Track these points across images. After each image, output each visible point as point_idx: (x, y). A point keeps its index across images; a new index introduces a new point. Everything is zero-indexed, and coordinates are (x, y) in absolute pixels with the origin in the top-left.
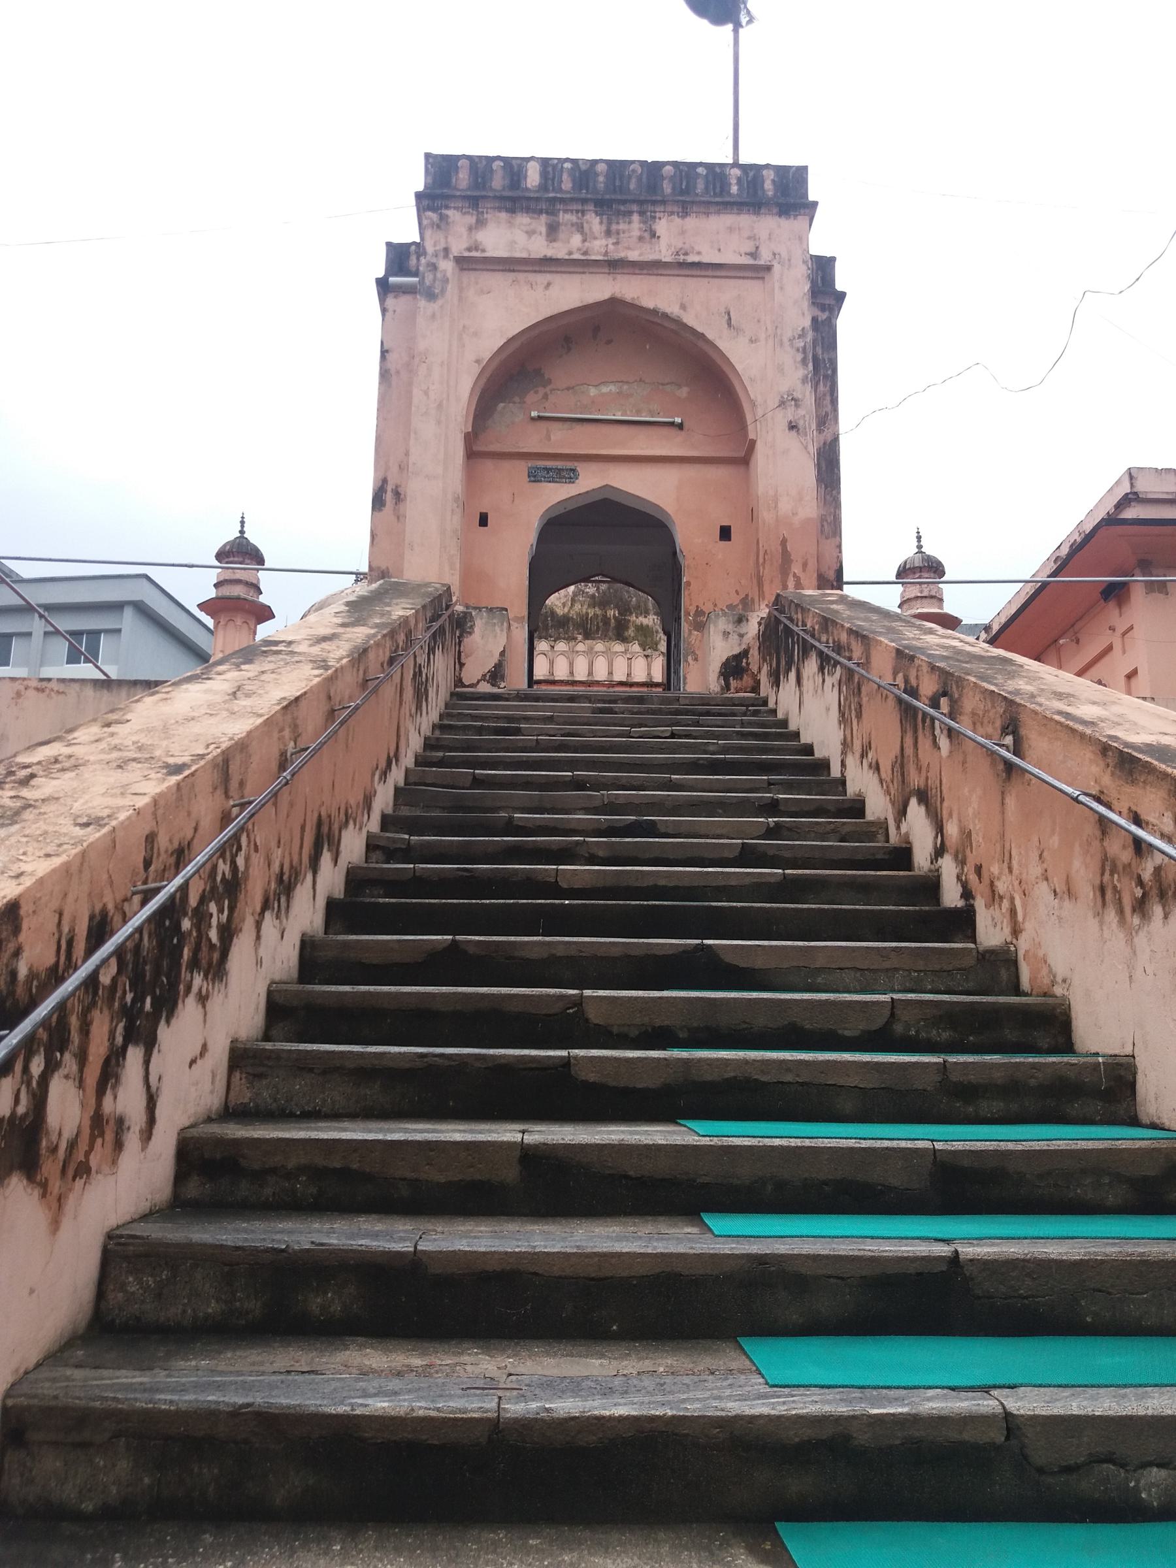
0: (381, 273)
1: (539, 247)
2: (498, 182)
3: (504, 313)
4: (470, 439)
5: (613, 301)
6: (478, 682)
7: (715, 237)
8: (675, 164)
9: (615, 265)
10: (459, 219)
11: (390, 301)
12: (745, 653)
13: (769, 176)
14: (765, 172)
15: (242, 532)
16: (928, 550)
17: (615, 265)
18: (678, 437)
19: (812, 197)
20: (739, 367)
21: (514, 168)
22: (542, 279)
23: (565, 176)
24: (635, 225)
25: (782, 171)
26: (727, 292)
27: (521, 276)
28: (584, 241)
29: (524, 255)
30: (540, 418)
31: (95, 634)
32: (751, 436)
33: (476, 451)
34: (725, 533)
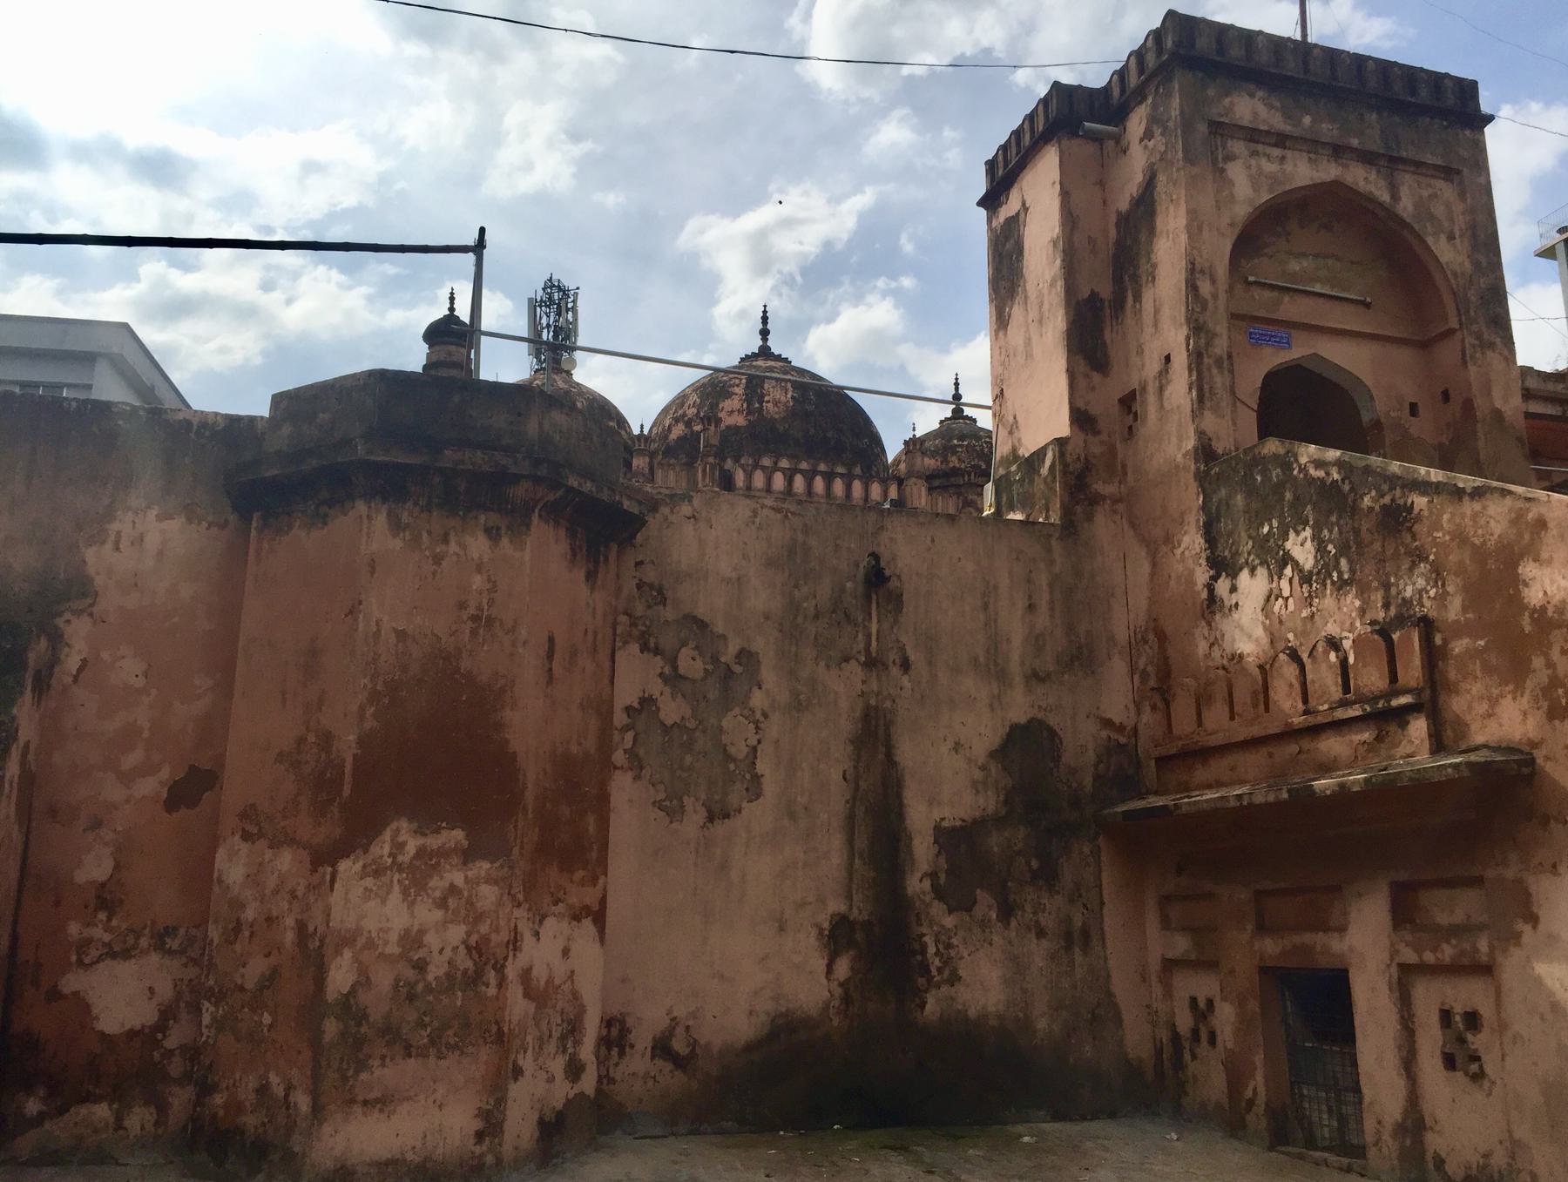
1: (1277, 122)
5: (1336, 184)
9: (1338, 151)
27: (1260, 147)
28: (1314, 121)
29: (1265, 128)
30: (1255, 282)
32: (1454, 324)
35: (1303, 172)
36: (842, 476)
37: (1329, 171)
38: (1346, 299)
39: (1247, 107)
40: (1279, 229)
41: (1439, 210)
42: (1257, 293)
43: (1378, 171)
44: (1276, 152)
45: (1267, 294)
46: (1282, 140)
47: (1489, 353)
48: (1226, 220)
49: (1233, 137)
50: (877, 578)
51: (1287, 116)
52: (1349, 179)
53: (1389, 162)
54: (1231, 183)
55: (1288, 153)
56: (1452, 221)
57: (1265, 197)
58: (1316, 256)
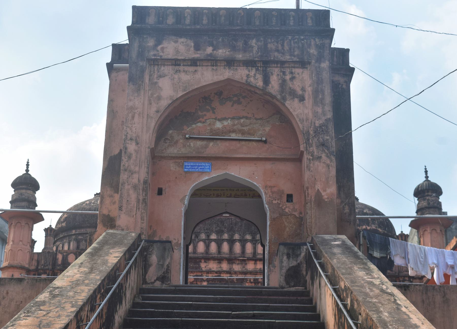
0: (109, 60)
4: (153, 151)
5: (229, 81)
6: (155, 281)
9: (230, 63)
11: (114, 74)
12: (299, 265)
14: (307, 14)
15: (27, 170)
16: (432, 179)
19: (331, 27)
20: (294, 114)
23: (205, 18)
27: (181, 68)
28: (213, 50)
29: (183, 58)
30: (191, 138)
35: (207, 77)
36: (240, 241)
37: (225, 74)
38: (253, 140)
40: (207, 107)
41: (296, 86)
42: (192, 143)
43: (257, 70)
44: (192, 69)
45: (199, 143)
46: (194, 62)
47: (317, 163)
48: (154, 109)
49: (164, 65)
51: (197, 48)
52: (237, 77)
53: (264, 64)
54: (161, 89)
55: (199, 68)
56: (303, 89)
57: (180, 94)
58: (233, 118)
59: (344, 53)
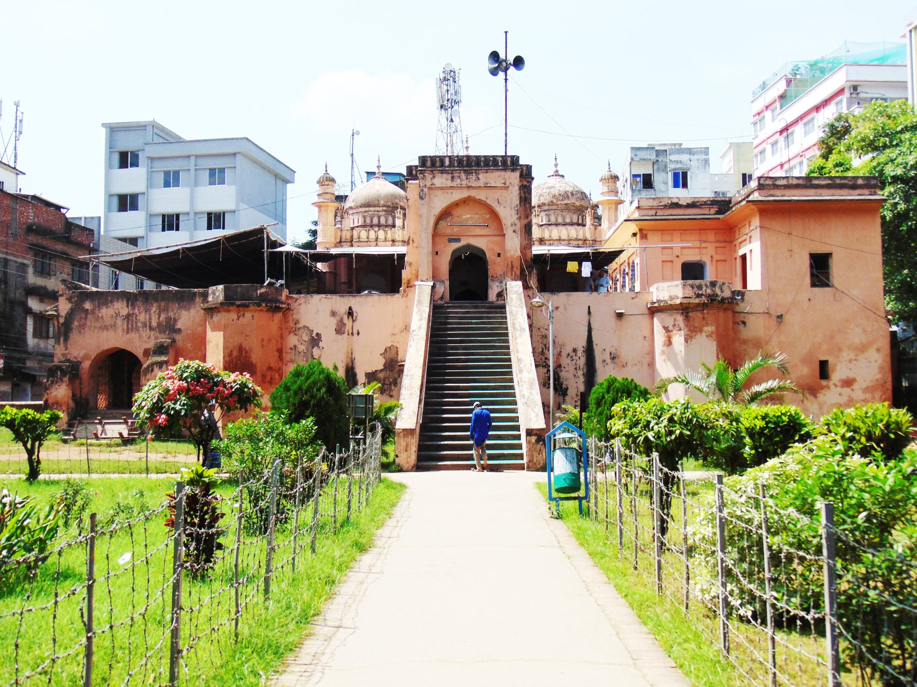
1: (449, 183)
2: (438, 164)
3: (440, 202)
7: (495, 178)
8: (484, 156)
9: (469, 187)
10: (428, 176)
13: (509, 159)
17: (469, 187)
18: (487, 229)
21: (442, 159)
22: (450, 191)
24: (474, 177)
25: (512, 157)
26: (497, 194)
31: (222, 171)
33: (435, 235)
34: (499, 255)
35: (457, 196)
39: (441, 180)
50: (350, 313)
59: (529, 168)
